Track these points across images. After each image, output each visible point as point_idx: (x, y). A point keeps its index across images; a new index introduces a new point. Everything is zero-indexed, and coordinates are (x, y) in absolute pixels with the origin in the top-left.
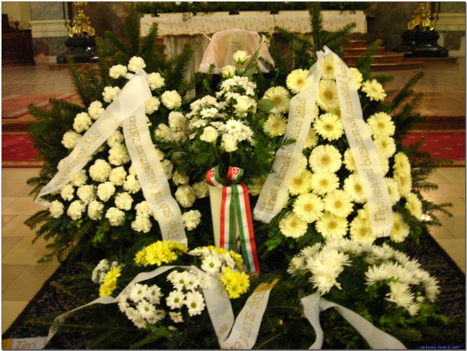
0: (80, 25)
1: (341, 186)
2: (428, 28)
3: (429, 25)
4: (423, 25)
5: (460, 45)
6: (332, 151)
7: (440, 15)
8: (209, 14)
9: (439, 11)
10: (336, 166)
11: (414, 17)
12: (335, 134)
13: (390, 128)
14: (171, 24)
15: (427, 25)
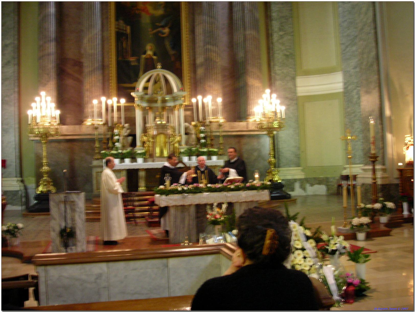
0: (45, 185)
1: (305, 261)
2: (277, 181)
3: (277, 179)
4: (274, 179)
5: (294, 188)
6: (300, 252)
7: (280, 169)
8: (194, 195)
9: (279, 167)
10: (302, 256)
11: (267, 175)
12: (299, 247)
13: (314, 244)
14: (175, 200)
15: (276, 179)
